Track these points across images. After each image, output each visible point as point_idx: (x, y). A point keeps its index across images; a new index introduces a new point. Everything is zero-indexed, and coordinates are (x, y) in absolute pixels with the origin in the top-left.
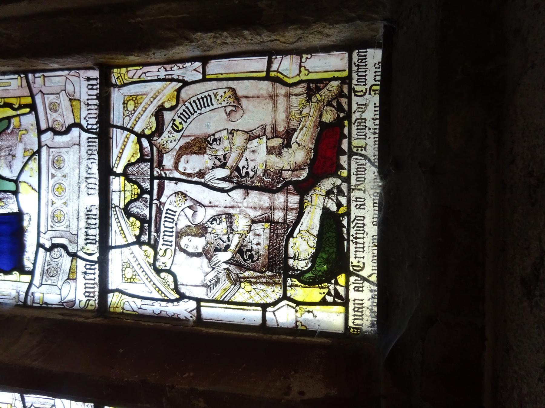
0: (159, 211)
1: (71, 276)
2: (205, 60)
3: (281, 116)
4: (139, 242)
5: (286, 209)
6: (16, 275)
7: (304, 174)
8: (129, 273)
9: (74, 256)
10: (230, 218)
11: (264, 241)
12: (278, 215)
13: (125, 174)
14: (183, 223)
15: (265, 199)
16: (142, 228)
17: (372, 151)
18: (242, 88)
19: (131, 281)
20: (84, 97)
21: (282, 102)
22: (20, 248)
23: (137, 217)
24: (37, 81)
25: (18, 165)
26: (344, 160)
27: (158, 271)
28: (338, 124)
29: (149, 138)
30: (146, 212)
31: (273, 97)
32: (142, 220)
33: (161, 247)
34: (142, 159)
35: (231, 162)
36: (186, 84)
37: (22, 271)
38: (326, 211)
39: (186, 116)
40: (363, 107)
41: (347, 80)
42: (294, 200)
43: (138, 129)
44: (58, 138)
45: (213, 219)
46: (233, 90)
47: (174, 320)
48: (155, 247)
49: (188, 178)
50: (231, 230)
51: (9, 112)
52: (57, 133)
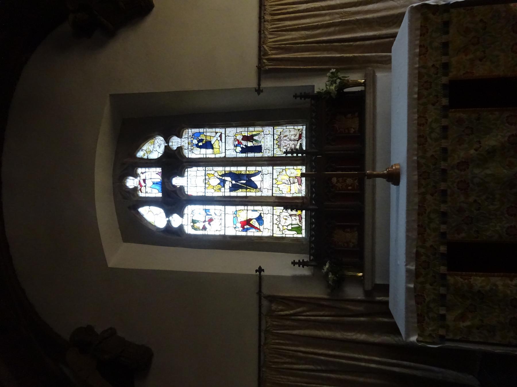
0: (281, 144)
1: (269, 152)
2: (286, 127)
3: (295, 133)
4: (278, 148)
5: (296, 143)
6: (261, 153)
7: (298, 139)
8: (277, 152)
9: (269, 150)
10: (289, 144)
11: (294, 147)
12: (295, 144)
13: (276, 140)
14: (284, 145)
15: (293, 142)
16: (278, 146)
17: (305, 137)
18: (291, 130)
19: (277, 152)
20: (270, 131)
21: (295, 131)
22: (262, 150)
23: (278, 145)
24: (264, 128)
25: (261, 139)
26: (302, 138)
27: (281, 151)
28: (301, 134)
29: (279, 135)
30: (279, 144)
31: (294, 131)
32: (279, 145)
33: (281, 148)
34: (278, 138)
35: (289, 138)
36: (284, 129)
37: (262, 152)
38: (300, 143)
39: (284, 133)
40: (304, 132)
41: (302, 129)
42: (297, 142)
43: (278, 134)
44: (267, 136)
45: (287, 145)
46: (290, 130)
47: (283, 157)
48: (280, 148)
49: (284, 140)
50: (290, 146)
51: (259, 132)
52: (267, 135)
